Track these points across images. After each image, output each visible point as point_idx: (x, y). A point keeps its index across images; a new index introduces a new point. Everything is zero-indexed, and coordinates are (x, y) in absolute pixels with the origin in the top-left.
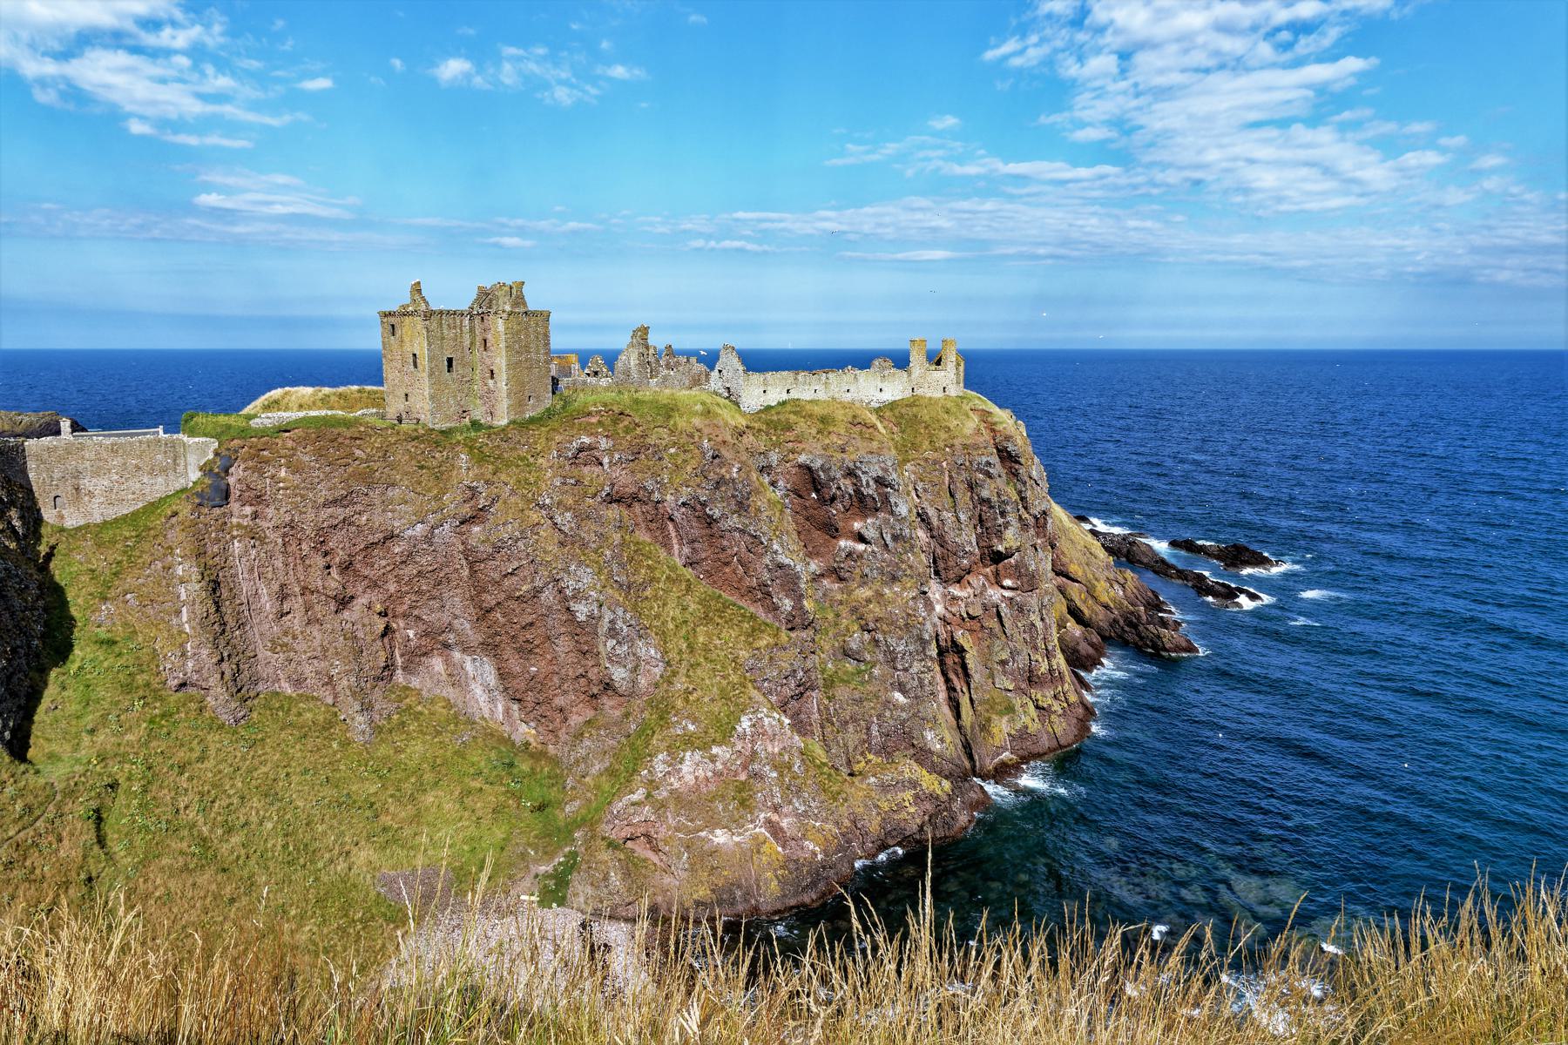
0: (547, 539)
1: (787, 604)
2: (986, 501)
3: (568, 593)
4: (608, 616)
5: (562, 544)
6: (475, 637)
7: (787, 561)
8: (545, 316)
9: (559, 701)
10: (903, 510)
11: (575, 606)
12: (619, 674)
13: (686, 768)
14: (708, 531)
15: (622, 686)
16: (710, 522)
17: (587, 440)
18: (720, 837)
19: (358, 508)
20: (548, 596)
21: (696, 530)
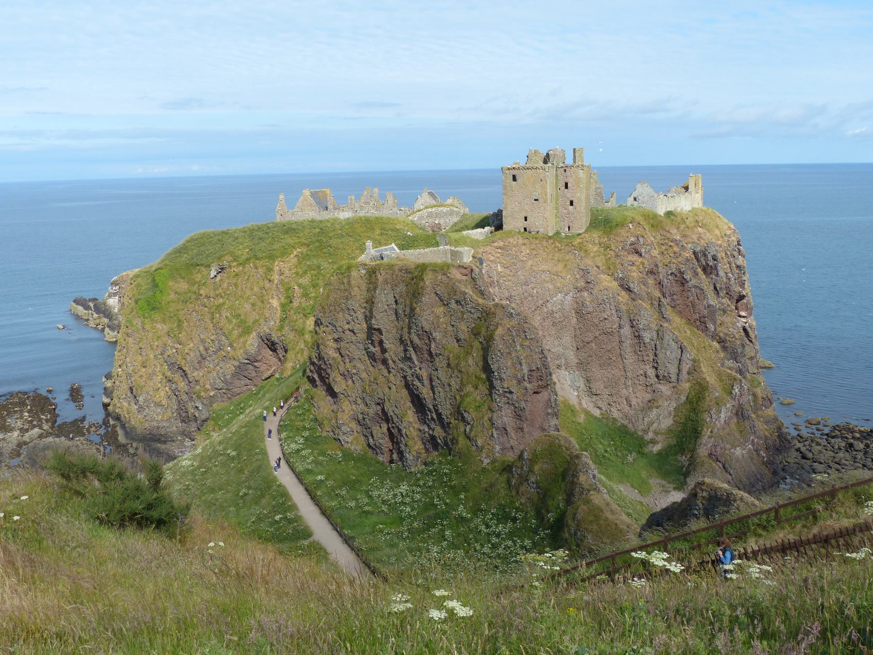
0: (624, 297)
2: (738, 267)
4: (667, 337)
5: (633, 299)
7: (712, 303)
10: (721, 273)
11: (642, 333)
13: (723, 415)
14: (681, 288)
15: (674, 378)
16: (683, 282)
17: (633, 239)
18: (738, 452)
19: (532, 285)
20: (626, 331)
21: (676, 288)
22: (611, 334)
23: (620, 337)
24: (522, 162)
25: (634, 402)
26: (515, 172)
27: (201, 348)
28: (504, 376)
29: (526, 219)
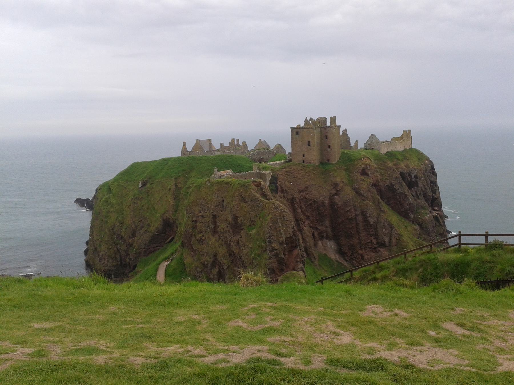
1: (412, 216)
2: (431, 182)
3: (368, 215)
6: (330, 234)
8: (339, 127)
9: (360, 252)
10: (420, 185)
12: (387, 240)
15: (387, 243)
20: (360, 218)
22: (351, 219)
23: (356, 221)
24: (302, 125)
25: (366, 257)
26: (298, 130)
27: (133, 226)
28: (272, 240)
29: (304, 156)
